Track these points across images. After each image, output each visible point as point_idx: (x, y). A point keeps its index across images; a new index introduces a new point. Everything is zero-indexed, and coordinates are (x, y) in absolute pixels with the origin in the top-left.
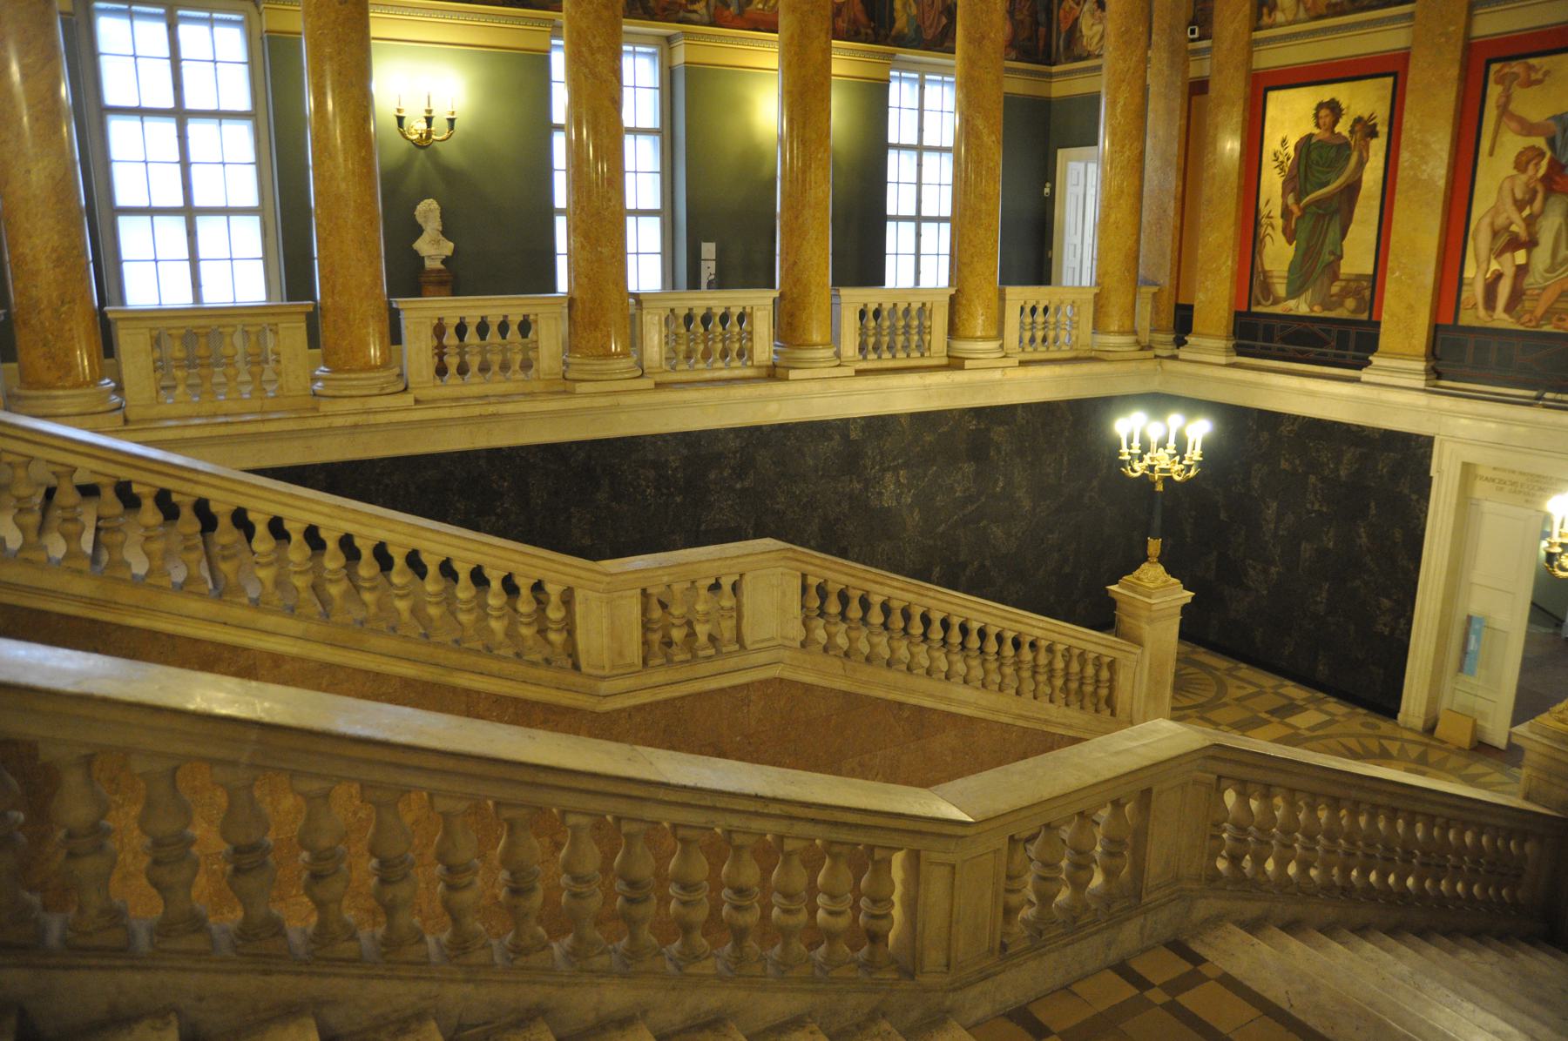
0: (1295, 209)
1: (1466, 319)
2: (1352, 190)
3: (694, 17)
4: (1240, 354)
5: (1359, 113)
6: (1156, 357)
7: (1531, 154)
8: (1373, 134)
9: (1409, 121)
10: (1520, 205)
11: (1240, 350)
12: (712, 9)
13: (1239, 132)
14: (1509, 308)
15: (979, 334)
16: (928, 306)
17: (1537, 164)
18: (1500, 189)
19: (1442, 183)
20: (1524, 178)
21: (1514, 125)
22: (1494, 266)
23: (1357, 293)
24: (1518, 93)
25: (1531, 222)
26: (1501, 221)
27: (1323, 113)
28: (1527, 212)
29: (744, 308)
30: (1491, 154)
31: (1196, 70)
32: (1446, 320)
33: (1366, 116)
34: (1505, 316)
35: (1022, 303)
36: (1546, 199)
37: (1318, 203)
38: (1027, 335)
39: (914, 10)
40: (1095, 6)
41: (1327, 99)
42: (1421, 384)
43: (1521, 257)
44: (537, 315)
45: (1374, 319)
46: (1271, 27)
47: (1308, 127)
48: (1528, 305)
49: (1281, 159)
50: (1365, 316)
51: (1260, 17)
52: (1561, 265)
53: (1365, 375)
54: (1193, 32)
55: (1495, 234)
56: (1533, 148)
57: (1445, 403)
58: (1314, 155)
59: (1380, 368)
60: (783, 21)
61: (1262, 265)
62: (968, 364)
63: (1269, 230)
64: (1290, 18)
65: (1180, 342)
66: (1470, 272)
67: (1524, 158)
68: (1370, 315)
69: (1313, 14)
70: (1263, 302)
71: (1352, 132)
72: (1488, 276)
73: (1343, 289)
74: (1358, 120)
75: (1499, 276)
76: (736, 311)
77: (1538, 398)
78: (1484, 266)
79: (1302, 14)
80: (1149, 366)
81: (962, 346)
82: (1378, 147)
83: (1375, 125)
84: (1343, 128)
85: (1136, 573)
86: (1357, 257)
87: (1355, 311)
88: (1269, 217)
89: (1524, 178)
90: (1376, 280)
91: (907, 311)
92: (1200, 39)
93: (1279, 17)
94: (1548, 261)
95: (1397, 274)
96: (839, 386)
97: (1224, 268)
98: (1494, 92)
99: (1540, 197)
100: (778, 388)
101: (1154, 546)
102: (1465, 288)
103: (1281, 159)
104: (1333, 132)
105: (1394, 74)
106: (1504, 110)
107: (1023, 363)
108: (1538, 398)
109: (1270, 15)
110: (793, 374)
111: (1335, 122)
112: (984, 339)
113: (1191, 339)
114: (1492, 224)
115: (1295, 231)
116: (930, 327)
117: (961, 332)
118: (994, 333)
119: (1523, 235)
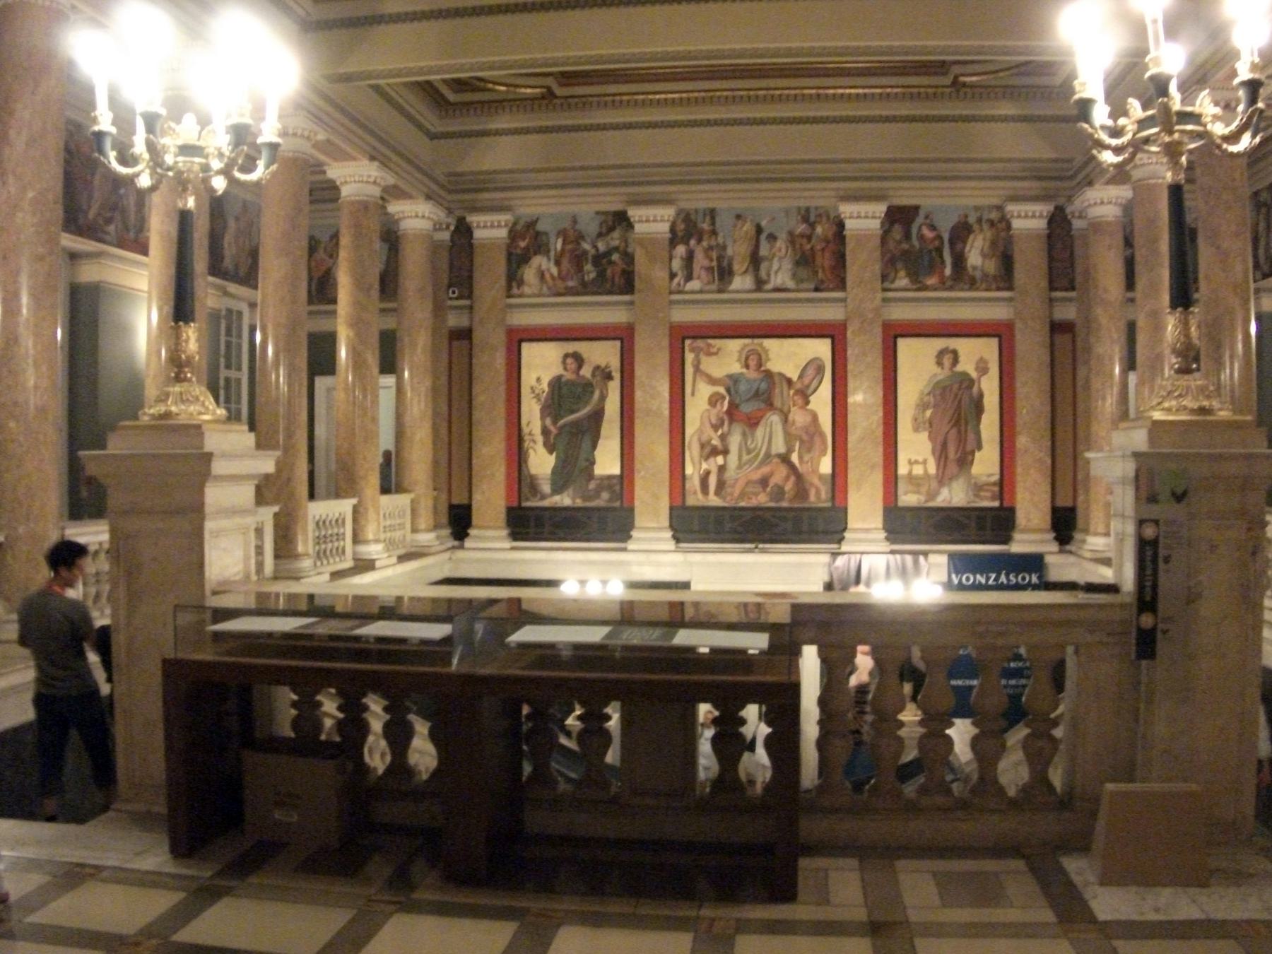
0: (553, 430)
1: (691, 501)
2: (598, 416)
8: (609, 377)
9: (640, 371)
10: (715, 428)
11: (515, 536)
14: (717, 493)
17: (722, 403)
18: (702, 417)
19: (667, 413)
20: (715, 411)
22: (704, 466)
23: (610, 488)
24: (704, 359)
25: (723, 438)
26: (704, 438)
27: (569, 361)
28: (720, 432)
30: (693, 394)
33: (603, 365)
34: (715, 498)
41: (571, 351)
42: (671, 545)
43: (720, 460)
46: (520, 296)
47: (557, 370)
48: (729, 490)
49: (537, 392)
50: (617, 504)
52: (745, 464)
53: (631, 545)
54: (454, 292)
55: (702, 446)
56: (717, 394)
58: (564, 391)
59: (638, 539)
61: (528, 470)
62: (378, 564)
63: (532, 444)
64: (536, 292)
66: (689, 470)
71: (593, 375)
74: (597, 368)
75: (708, 473)
78: (697, 466)
79: (545, 289)
82: (614, 388)
84: (586, 372)
86: (607, 462)
87: (610, 500)
88: (530, 434)
89: (715, 411)
92: (457, 299)
93: (526, 290)
94: (737, 463)
95: (643, 473)
97: (497, 474)
98: (689, 357)
103: (537, 392)
106: (697, 369)
108: (756, 548)
109: (518, 287)
111: (580, 367)
113: (472, 532)
114: (699, 439)
117: (361, 537)
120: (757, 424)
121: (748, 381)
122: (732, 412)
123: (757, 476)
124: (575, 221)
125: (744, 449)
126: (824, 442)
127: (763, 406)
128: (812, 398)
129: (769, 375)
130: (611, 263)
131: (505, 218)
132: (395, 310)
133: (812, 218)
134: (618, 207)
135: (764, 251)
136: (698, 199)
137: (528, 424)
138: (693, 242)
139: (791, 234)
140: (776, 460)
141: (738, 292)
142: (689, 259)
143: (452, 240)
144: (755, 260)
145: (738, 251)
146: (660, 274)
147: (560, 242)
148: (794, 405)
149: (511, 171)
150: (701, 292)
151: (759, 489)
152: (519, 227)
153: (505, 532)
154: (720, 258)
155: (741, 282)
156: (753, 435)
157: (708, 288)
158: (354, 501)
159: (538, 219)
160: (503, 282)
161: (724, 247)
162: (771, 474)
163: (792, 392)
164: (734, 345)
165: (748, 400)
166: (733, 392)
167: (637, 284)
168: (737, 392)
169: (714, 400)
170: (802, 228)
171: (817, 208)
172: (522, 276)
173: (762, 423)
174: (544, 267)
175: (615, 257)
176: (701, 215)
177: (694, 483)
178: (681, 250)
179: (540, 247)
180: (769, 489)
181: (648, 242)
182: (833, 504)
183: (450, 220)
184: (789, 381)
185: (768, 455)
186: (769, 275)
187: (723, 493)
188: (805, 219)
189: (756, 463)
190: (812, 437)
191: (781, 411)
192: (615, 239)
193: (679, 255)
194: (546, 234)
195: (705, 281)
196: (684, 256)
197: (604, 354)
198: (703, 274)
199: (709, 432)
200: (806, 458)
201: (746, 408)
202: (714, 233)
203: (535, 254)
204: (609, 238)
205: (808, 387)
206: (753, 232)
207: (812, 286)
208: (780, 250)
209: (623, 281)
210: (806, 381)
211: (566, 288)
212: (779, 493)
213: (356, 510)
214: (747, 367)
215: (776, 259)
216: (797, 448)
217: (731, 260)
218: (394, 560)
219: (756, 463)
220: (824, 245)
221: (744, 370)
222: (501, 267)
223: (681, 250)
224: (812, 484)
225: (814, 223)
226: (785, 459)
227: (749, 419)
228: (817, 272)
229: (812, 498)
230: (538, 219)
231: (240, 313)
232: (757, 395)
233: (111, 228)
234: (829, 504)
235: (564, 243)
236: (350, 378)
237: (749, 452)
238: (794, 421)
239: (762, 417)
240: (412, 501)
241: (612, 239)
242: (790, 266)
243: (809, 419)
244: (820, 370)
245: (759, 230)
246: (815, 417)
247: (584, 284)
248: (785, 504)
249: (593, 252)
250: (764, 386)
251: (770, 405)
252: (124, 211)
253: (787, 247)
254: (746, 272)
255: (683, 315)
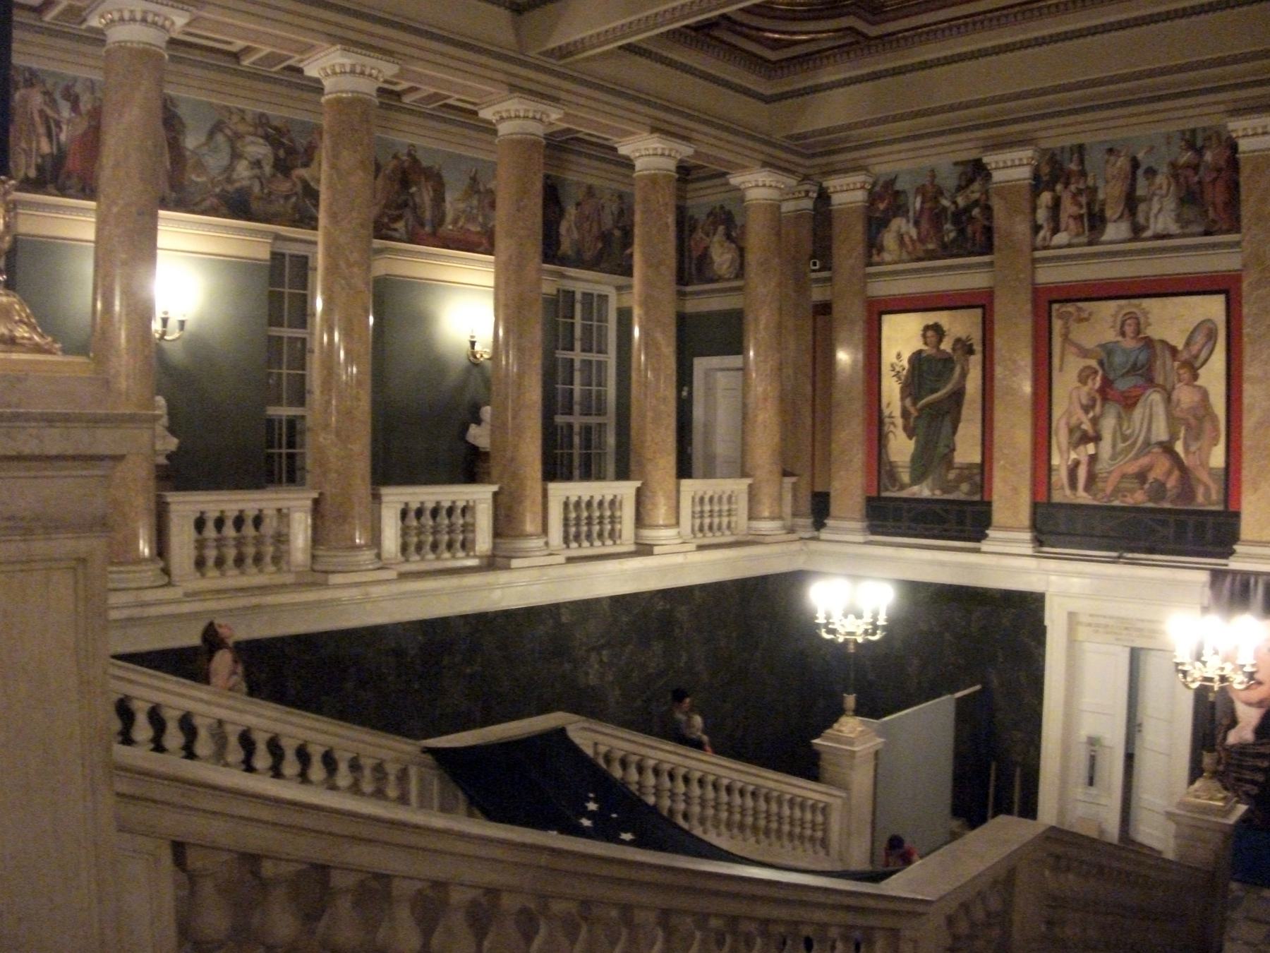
0: (912, 410)
1: (1057, 497)
2: (958, 396)
3: (397, 235)
4: (874, 533)
5: (959, 335)
6: (801, 539)
7: (1088, 372)
8: (971, 351)
9: (999, 342)
10: (1086, 409)
11: (873, 530)
12: (410, 228)
13: (861, 346)
14: (1087, 488)
15: (661, 522)
16: (619, 498)
17: (1094, 379)
20: (1086, 389)
21: (1073, 350)
22: (1073, 456)
24: (1074, 326)
25: (1095, 421)
26: (1074, 421)
27: (930, 333)
28: (1091, 415)
29: (468, 502)
30: (1061, 370)
31: (817, 294)
32: (1042, 499)
33: (964, 337)
35: (692, 494)
36: (1103, 406)
37: (930, 405)
38: (698, 522)
39: (576, 235)
40: (724, 239)
41: (931, 323)
42: (1030, 551)
43: (1091, 449)
44: (288, 509)
45: (986, 499)
46: (879, 264)
47: (918, 344)
48: (1100, 485)
49: (898, 369)
50: (977, 498)
51: (870, 256)
52: (1120, 454)
53: (984, 546)
55: (1071, 431)
56: (1089, 367)
57: (1052, 564)
58: (925, 367)
59: (995, 540)
60: (501, 243)
62: (656, 550)
63: (892, 428)
64: (896, 258)
65: (819, 524)
66: (1056, 460)
67: (1084, 374)
68: (982, 497)
69: (914, 257)
70: (890, 488)
71: (954, 349)
72: (1070, 463)
73: (959, 475)
74: (958, 341)
75: (1077, 464)
76: (461, 504)
77: (1119, 557)
79: (905, 256)
80: (796, 546)
81: (649, 534)
82: (975, 361)
83: (971, 345)
84: (946, 346)
85: (836, 726)
86: (967, 451)
87: (970, 493)
88: (890, 417)
89: (1086, 389)
90: (985, 467)
91: (601, 504)
92: (819, 270)
93: (887, 257)
95: (1002, 462)
96: (553, 572)
97: (855, 460)
98: (1057, 325)
99: (1099, 403)
100: (503, 577)
101: (850, 700)
102: (1053, 473)
103: (898, 369)
104: (938, 349)
105: (983, 307)
106: (1066, 337)
107: (701, 548)
108: (1119, 557)
110: (515, 563)
111: (940, 341)
112: (666, 526)
113: (830, 522)
114: (1068, 424)
115: (914, 428)
116: (621, 517)
117: (647, 521)
118: (673, 521)
119: (1091, 432)
120: (1135, 404)
121: (1124, 351)
122: (1105, 391)
123: (1133, 468)
124: (933, 174)
125: (1118, 434)
126: (1216, 429)
127: (1141, 381)
128: (1201, 372)
129: (1149, 343)
130: (971, 219)
131: (859, 178)
132: (739, 289)
133: (1199, 143)
134: (973, 155)
135: (1140, 192)
136: (1058, 136)
137: (889, 405)
138: (1059, 187)
139: (1173, 165)
140: (1156, 450)
141: (1111, 242)
142: (1056, 206)
143: (815, 209)
144: (1131, 203)
145: (1110, 192)
146: (1022, 228)
147: (919, 200)
148: (1180, 381)
149: (849, 127)
150: (1069, 245)
151: (1135, 484)
152: (877, 189)
153: (859, 525)
154: (1089, 205)
155: (1115, 231)
156: (1129, 420)
157: (1075, 241)
158: (638, 484)
159: (896, 177)
160: (861, 249)
161: (1093, 191)
162: (1150, 468)
163: (1176, 364)
164: (1108, 309)
165: (1123, 376)
166: (1106, 365)
167: (996, 242)
168: (1111, 364)
169: (1084, 377)
170: (1187, 157)
171: (1204, 129)
172: (882, 241)
173: (1140, 405)
174: (904, 230)
175: (976, 212)
176: (1067, 155)
177: (1061, 476)
178: (1046, 197)
179: (899, 207)
180: (1147, 486)
181: (1007, 190)
182: (1226, 506)
183: (807, 187)
184: (1174, 351)
185: (1147, 443)
186: (1147, 219)
187: (1094, 487)
188: (1191, 145)
189: (1131, 455)
190: (1200, 420)
191: (1163, 388)
192: (975, 191)
193: (1043, 205)
194: (904, 192)
195: (1073, 233)
196: (1050, 204)
197: (959, 325)
198: (1071, 222)
199: (1080, 414)
200: (1193, 449)
201: (1122, 385)
202: (1083, 174)
203: (895, 216)
204: (968, 191)
205: (1196, 357)
206: (1128, 167)
207: (1201, 229)
208: (1160, 188)
209: (983, 239)
210: (1194, 349)
211: (927, 251)
212: (1159, 491)
213: (639, 493)
214: (1123, 334)
215: (1156, 199)
216: (1182, 435)
217: (1103, 203)
218: (692, 547)
219: (1131, 455)
220: (1214, 175)
221: (1120, 338)
222: (858, 232)
223: (1046, 197)
224: (1199, 481)
225: (1203, 147)
226: (1167, 448)
227: (1126, 398)
228: (1206, 211)
229: (1200, 498)
230: (896, 177)
231: (603, 298)
232: (1134, 369)
233: (400, 225)
234: (1220, 508)
235: (923, 202)
236: (643, 358)
237: (1125, 438)
238: (1179, 401)
239: (1141, 395)
240: (750, 486)
241: (973, 192)
242: (1173, 206)
243: (1197, 398)
244: (1211, 336)
245: (1135, 164)
246: (1205, 394)
247: (944, 246)
248: (1167, 505)
249: (953, 208)
250: (1142, 357)
251: (1150, 382)
252: (415, 208)
253: (1169, 185)
254: (1121, 217)
255: (1048, 275)
